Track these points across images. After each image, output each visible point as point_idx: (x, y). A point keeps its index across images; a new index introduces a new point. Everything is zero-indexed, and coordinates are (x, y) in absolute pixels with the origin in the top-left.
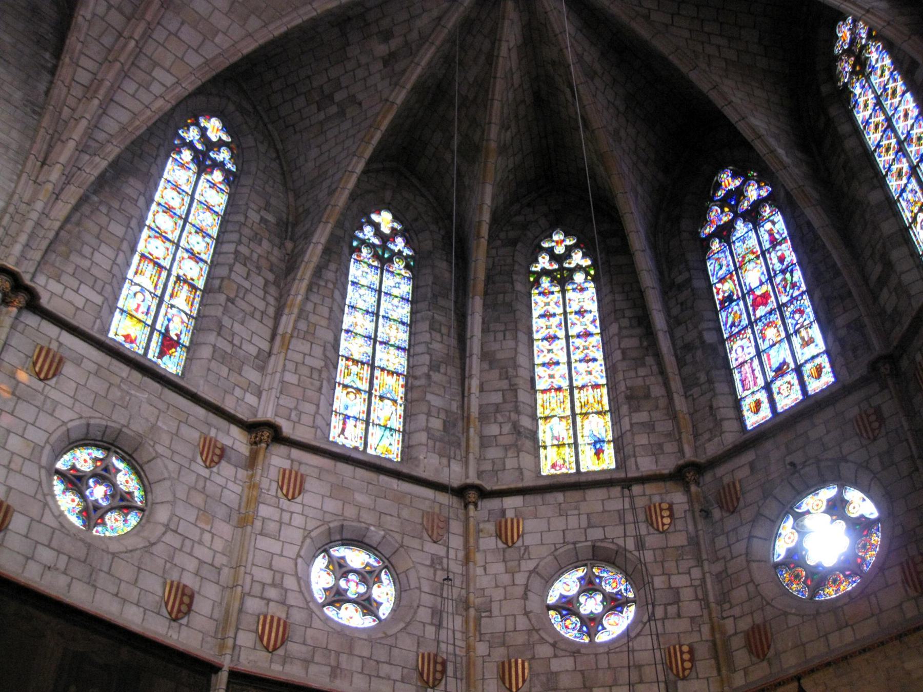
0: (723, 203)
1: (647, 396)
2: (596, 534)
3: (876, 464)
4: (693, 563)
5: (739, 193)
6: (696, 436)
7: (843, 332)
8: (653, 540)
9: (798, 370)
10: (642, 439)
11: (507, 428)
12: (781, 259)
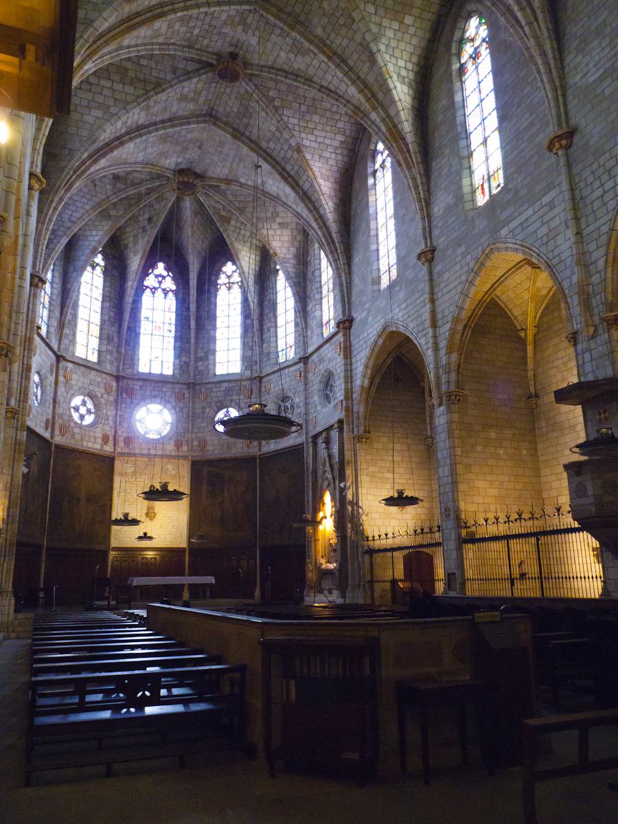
1: (113, 340)
3: (178, 409)
5: (164, 278)
6: (124, 364)
7: (182, 363)
8: (105, 396)
9: (162, 362)
10: (108, 357)
11: (72, 333)
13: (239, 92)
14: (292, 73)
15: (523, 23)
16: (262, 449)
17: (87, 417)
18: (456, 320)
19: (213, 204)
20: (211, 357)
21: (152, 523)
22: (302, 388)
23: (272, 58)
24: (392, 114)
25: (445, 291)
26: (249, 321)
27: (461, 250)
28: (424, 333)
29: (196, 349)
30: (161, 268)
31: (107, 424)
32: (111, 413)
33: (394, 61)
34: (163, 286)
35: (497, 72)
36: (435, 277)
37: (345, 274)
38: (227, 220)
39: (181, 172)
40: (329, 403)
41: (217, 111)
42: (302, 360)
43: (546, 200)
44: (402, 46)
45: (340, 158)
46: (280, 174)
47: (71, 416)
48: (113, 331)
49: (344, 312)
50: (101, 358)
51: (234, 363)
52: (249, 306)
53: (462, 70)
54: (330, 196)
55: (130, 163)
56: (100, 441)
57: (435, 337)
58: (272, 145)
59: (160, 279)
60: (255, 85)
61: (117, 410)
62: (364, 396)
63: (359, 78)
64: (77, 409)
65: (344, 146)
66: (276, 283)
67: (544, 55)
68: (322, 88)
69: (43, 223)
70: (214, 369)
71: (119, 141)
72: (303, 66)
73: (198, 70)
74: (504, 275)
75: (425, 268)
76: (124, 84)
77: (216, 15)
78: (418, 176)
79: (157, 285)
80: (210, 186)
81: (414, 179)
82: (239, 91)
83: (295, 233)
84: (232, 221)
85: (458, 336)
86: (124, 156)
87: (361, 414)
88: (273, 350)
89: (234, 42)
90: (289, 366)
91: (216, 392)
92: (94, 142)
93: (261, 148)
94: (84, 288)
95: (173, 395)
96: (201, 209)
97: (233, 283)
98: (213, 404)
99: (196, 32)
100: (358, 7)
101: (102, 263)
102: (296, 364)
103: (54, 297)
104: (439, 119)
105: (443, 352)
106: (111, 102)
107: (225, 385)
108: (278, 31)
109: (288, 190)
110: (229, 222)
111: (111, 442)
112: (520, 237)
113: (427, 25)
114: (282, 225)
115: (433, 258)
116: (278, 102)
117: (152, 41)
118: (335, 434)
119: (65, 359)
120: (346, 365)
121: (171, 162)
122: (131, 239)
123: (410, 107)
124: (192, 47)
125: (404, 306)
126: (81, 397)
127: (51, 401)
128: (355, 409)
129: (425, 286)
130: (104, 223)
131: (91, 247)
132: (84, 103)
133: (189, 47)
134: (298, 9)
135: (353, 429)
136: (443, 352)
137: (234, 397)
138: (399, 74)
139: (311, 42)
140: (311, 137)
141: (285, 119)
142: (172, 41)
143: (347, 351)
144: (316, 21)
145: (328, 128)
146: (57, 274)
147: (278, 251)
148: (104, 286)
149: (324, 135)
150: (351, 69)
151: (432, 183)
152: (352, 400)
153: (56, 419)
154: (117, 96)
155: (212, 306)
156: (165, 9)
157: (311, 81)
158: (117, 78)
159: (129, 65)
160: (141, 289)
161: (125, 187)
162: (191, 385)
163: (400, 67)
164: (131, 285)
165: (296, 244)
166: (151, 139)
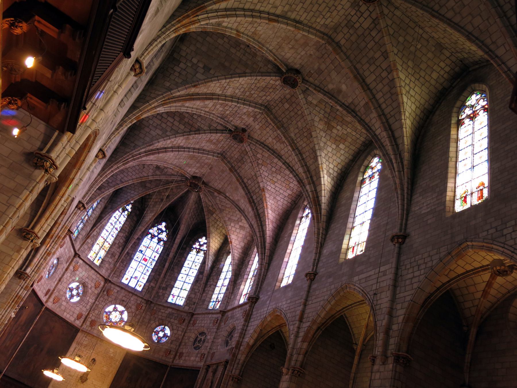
0: (158, 229)
1: (115, 256)
2: (87, 280)
4: (94, 298)
5: (162, 231)
6: (114, 274)
8: (93, 289)
9: (138, 281)
10: (107, 265)
11: (92, 243)
12: (155, 257)
13: (241, 149)
14: (272, 150)
15: (396, 170)
16: (175, 362)
17: (75, 297)
18: (314, 322)
19: (207, 201)
20: (169, 289)
21: (82, 385)
22: (215, 330)
23: (264, 139)
24: (318, 191)
25: (314, 301)
26: (201, 276)
27: (330, 280)
28: (294, 323)
29: (163, 281)
30: (163, 226)
31: (86, 307)
32: (91, 301)
33: (327, 163)
34: (160, 236)
35: (380, 189)
36: (311, 291)
37: (265, 269)
38: (211, 213)
39: (194, 177)
40: (227, 346)
41: (226, 154)
42: (222, 312)
43: (382, 269)
44: (335, 157)
45: (285, 202)
46: (249, 199)
47: (66, 293)
48: (117, 251)
49: (255, 292)
50: (102, 265)
51: (181, 298)
52: (205, 267)
53: (363, 182)
54: (272, 222)
55: (168, 163)
56: (75, 316)
57: (299, 328)
58: (249, 182)
59: (160, 232)
60: (251, 149)
61: (96, 300)
62: (247, 350)
63: (306, 165)
64: (71, 290)
65: (290, 197)
66: (226, 259)
67: (402, 190)
68: (285, 163)
69: (101, 177)
70: (168, 298)
71: (165, 150)
72: (279, 149)
73: (222, 130)
74: (351, 305)
75: (307, 283)
76: (180, 123)
77: (241, 108)
78: (321, 229)
79: (156, 234)
80: (209, 191)
81: (319, 229)
82: (241, 149)
83: (248, 234)
84: (214, 214)
85: (312, 333)
86: (166, 158)
87: (241, 361)
88: (207, 299)
89: (247, 124)
90: (212, 314)
91: (163, 313)
92: (150, 145)
93: (243, 181)
94: (113, 220)
95: (136, 304)
96: (199, 201)
97: (202, 250)
98: (157, 319)
99: (228, 112)
100: (316, 131)
101: (130, 210)
102: (217, 313)
103: (91, 219)
104: (343, 202)
105: (300, 340)
106: (169, 129)
107: (170, 310)
108: (271, 127)
109: (250, 209)
110: (212, 215)
111: (82, 320)
112: (363, 285)
113: (352, 152)
114: (242, 227)
115: (314, 279)
116: (260, 161)
117: (202, 109)
118: (221, 369)
119: (79, 257)
120: (244, 325)
121: (192, 171)
122: (153, 203)
123: (329, 190)
124: (223, 119)
125: (289, 301)
126: (77, 284)
127: (58, 279)
128: (239, 356)
129: (304, 294)
130: (141, 189)
131: (127, 199)
132: (155, 125)
133: (221, 118)
134: (285, 120)
135: (232, 370)
136: (300, 340)
137: (172, 320)
138: (328, 171)
139: (286, 139)
140: (273, 186)
141: (261, 171)
142: (213, 112)
143: (248, 317)
144: (292, 129)
145: (284, 185)
146: (99, 206)
147: (233, 241)
148: (125, 223)
149: (281, 187)
150: (303, 159)
151: (328, 236)
152: (239, 350)
153: (55, 291)
154: (174, 128)
155: (183, 259)
156: (214, 97)
157: (281, 158)
158: (178, 119)
159: (187, 115)
160: (146, 233)
161: (160, 174)
162: (149, 302)
163: (330, 168)
164: (141, 229)
165: (246, 241)
166: (184, 155)
